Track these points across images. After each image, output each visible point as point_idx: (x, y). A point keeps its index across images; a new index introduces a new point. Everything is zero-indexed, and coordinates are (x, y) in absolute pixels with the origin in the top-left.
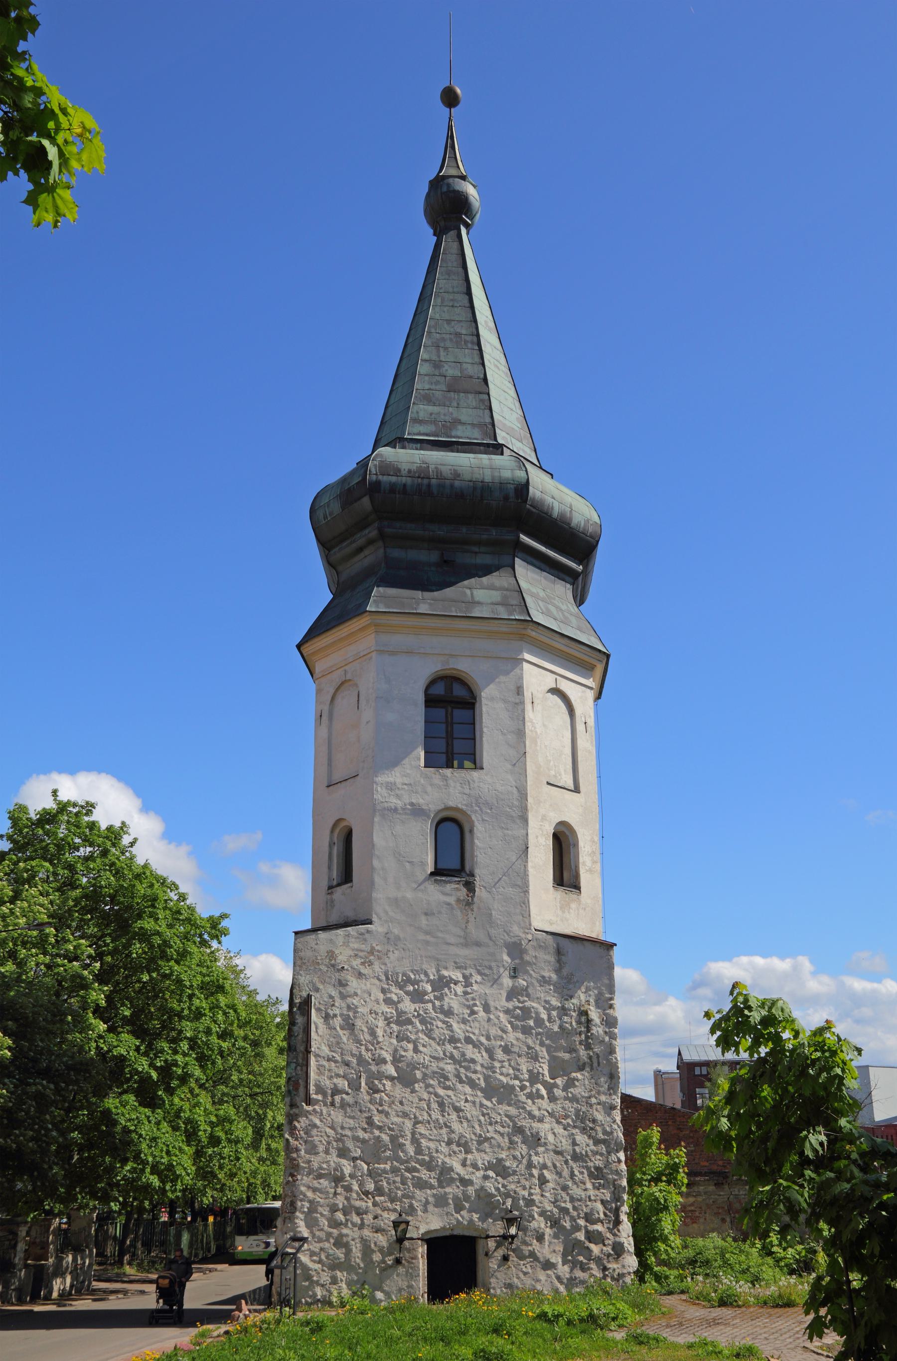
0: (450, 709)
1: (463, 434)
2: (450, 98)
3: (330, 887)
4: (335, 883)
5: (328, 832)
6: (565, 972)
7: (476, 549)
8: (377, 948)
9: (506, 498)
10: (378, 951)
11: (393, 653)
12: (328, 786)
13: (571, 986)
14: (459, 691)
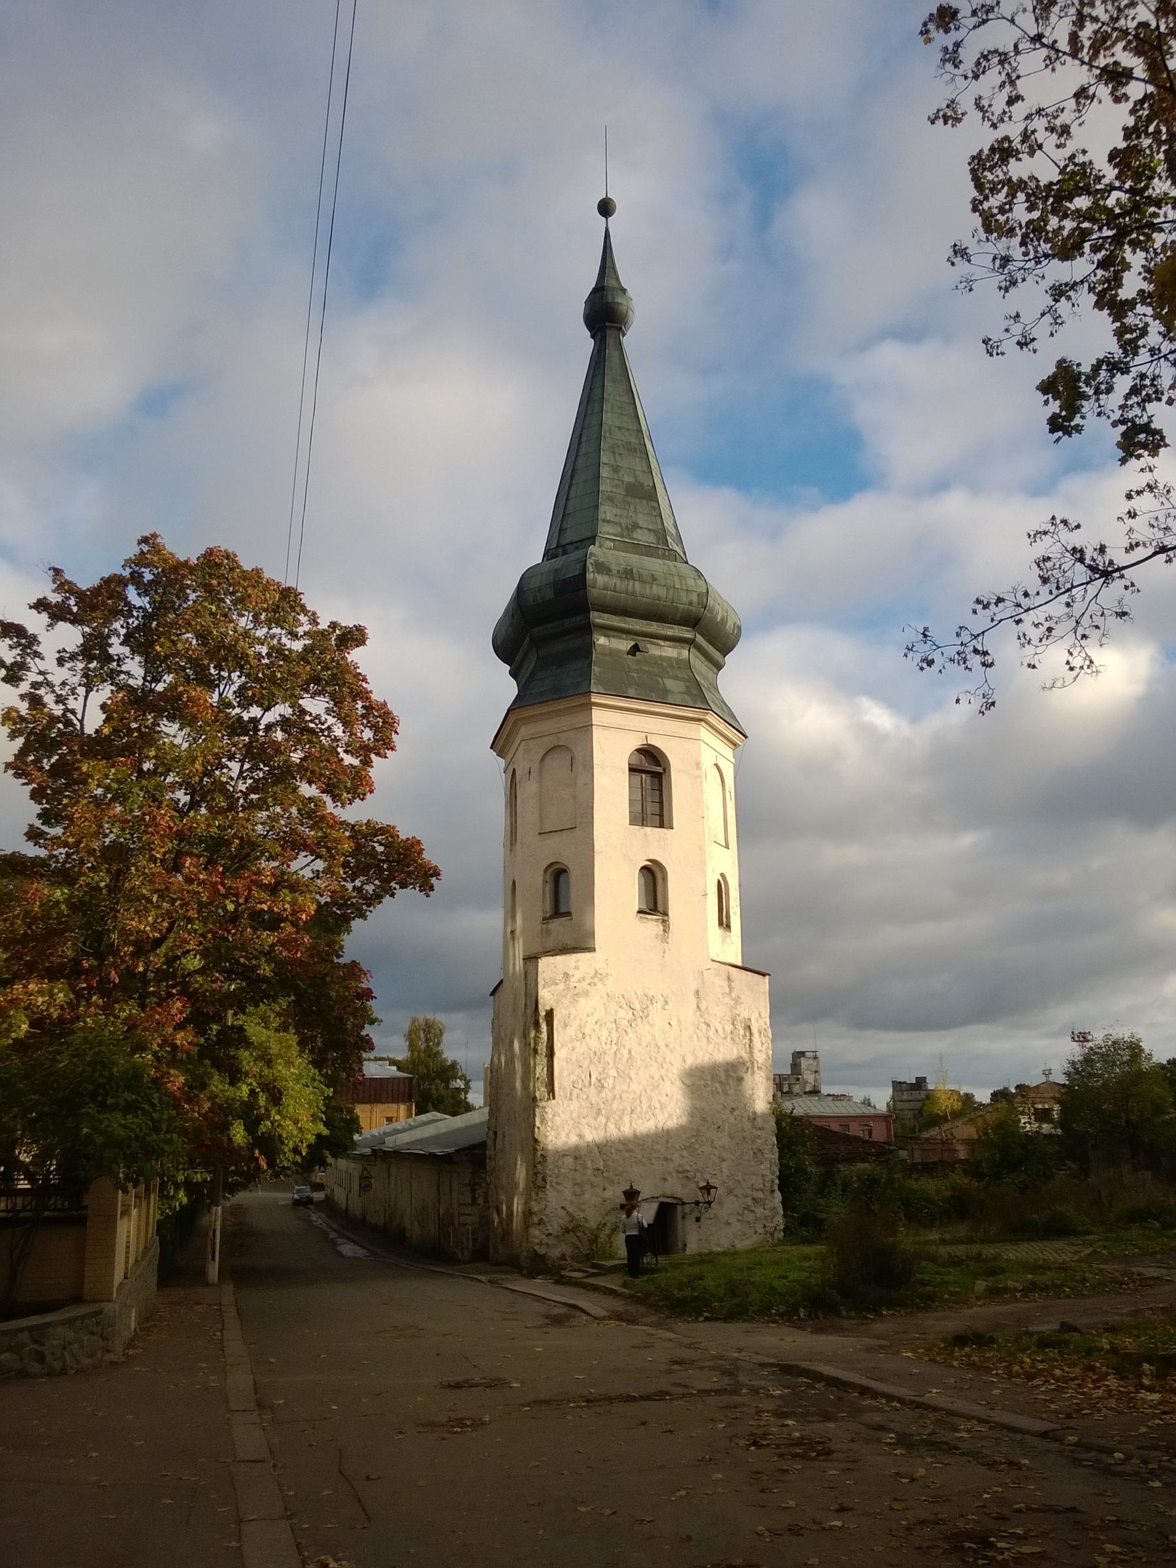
1: (643, 537)
6: (733, 995)
7: (662, 643)
9: (691, 604)
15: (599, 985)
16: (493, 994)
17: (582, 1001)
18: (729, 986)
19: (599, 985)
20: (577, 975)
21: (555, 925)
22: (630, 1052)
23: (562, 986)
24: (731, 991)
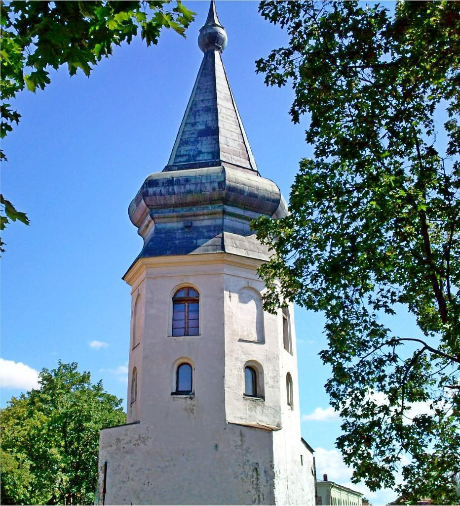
0: (187, 304)
1: (201, 158)
6: (244, 447)
7: (202, 218)
10: (143, 438)
11: (154, 278)
14: (192, 295)
15: (142, 445)
20: (127, 439)
24: (241, 446)
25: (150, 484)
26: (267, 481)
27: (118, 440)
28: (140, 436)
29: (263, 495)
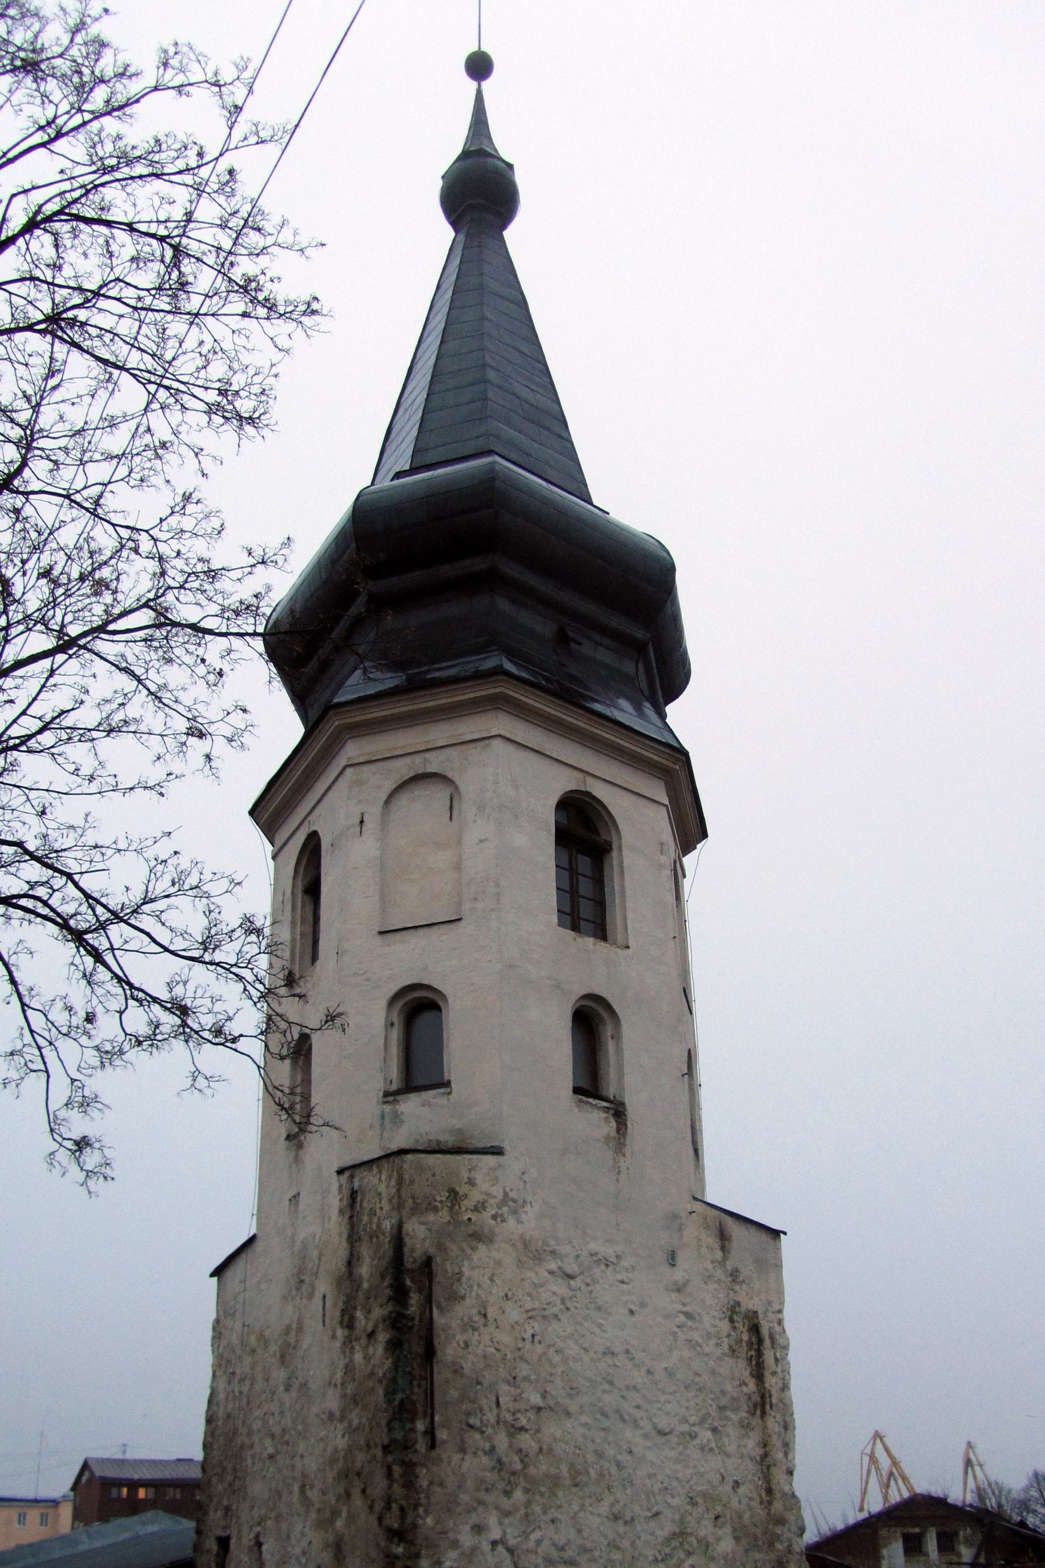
2: (479, 67)
3: (386, 1094)
4: (394, 1087)
5: (383, 1003)
7: (597, 637)
8: (512, 1195)
10: (514, 1201)
12: (381, 933)
13: (737, 1287)
16: (218, 1272)
17: (482, 1248)
18: (723, 1248)
19: (511, 1222)
20: (476, 1196)
21: (411, 1105)
22: (565, 1361)
23: (444, 1216)
24: (725, 1258)
25: (537, 1338)
26: (777, 1360)
27: (454, 1196)
28: (506, 1194)
29: (770, 1396)
